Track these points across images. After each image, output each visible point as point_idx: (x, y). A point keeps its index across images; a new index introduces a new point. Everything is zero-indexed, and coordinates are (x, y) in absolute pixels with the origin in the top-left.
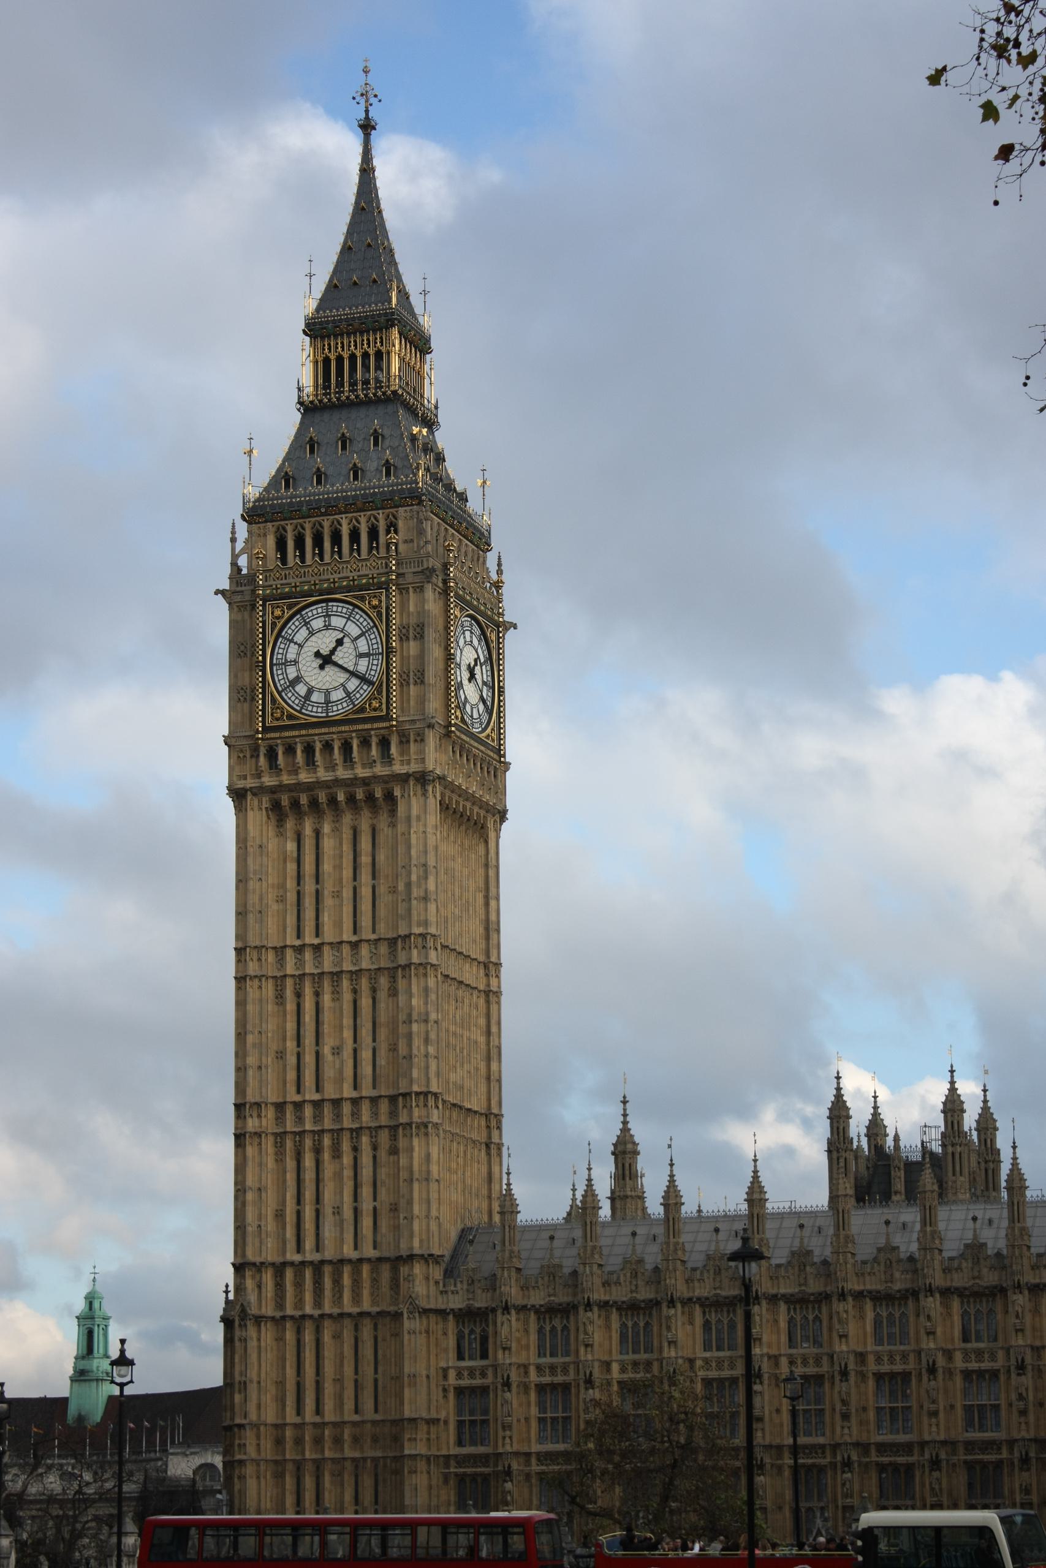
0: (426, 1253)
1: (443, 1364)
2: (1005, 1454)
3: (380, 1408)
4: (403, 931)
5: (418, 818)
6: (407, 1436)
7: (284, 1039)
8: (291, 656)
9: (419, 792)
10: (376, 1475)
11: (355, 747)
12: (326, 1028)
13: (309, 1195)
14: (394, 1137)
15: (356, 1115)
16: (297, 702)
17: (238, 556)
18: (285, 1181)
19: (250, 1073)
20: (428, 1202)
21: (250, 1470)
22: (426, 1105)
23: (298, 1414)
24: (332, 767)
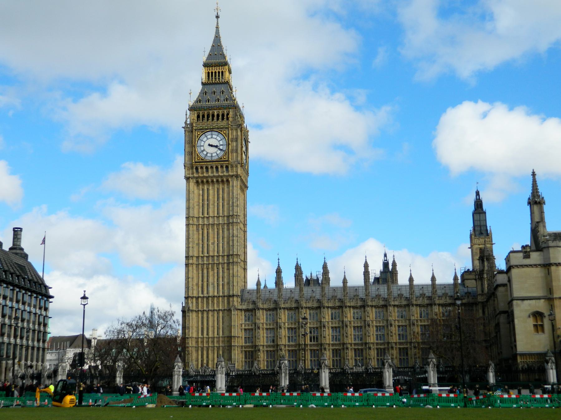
1: (241, 323)
2: (386, 346)
3: (224, 334)
6: (233, 341)
7: (199, 240)
8: (202, 144)
9: (236, 180)
10: (223, 351)
12: (211, 238)
13: (205, 280)
15: (218, 260)
19: (190, 248)
21: (190, 348)
22: (237, 258)
23: (202, 335)
24: (213, 172)
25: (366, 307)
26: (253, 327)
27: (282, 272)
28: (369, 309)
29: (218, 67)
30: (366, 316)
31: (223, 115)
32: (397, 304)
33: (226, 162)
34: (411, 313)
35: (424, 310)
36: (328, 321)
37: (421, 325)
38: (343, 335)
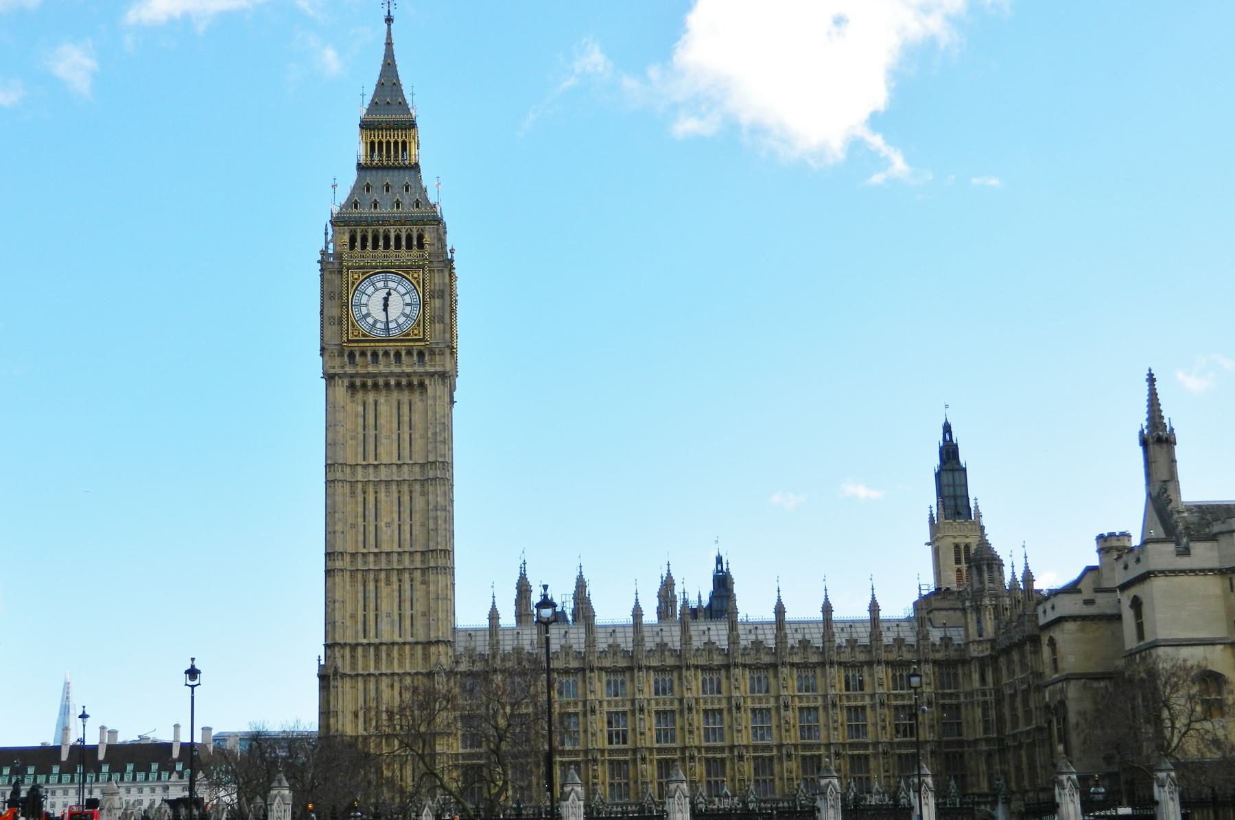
0: (446, 640)
2: (775, 752)
4: (431, 459)
5: (440, 397)
6: (437, 742)
7: (357, 517)
9: (441, 383)
11: (403, 354)
13: (372, 606)
14: (423, 574)
16: (367, 327)
17: (329, 243)
18: (357, 598)
19: (337, 535)
20: (447, 611)
24: (388, 365)
25: (732, 668)
26: (628, 707)
27: (532, 591)
28: (737, 672)
29: (394, 130)
30: (732, 687)
31: (409, 238)
32: (798, 661)
33: (420, 344)
34: (828, 681)
35: (854, 675)
36: (649, 698)
37: (849, 708)
38: (682, 729)
